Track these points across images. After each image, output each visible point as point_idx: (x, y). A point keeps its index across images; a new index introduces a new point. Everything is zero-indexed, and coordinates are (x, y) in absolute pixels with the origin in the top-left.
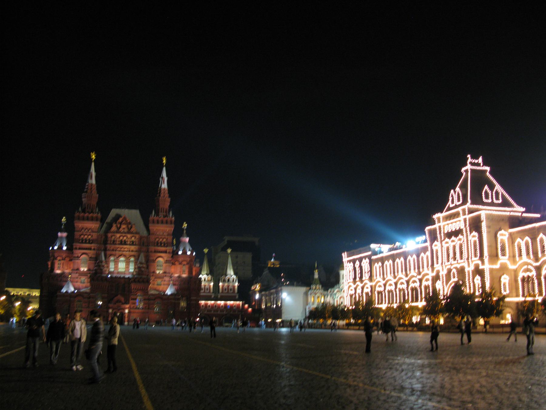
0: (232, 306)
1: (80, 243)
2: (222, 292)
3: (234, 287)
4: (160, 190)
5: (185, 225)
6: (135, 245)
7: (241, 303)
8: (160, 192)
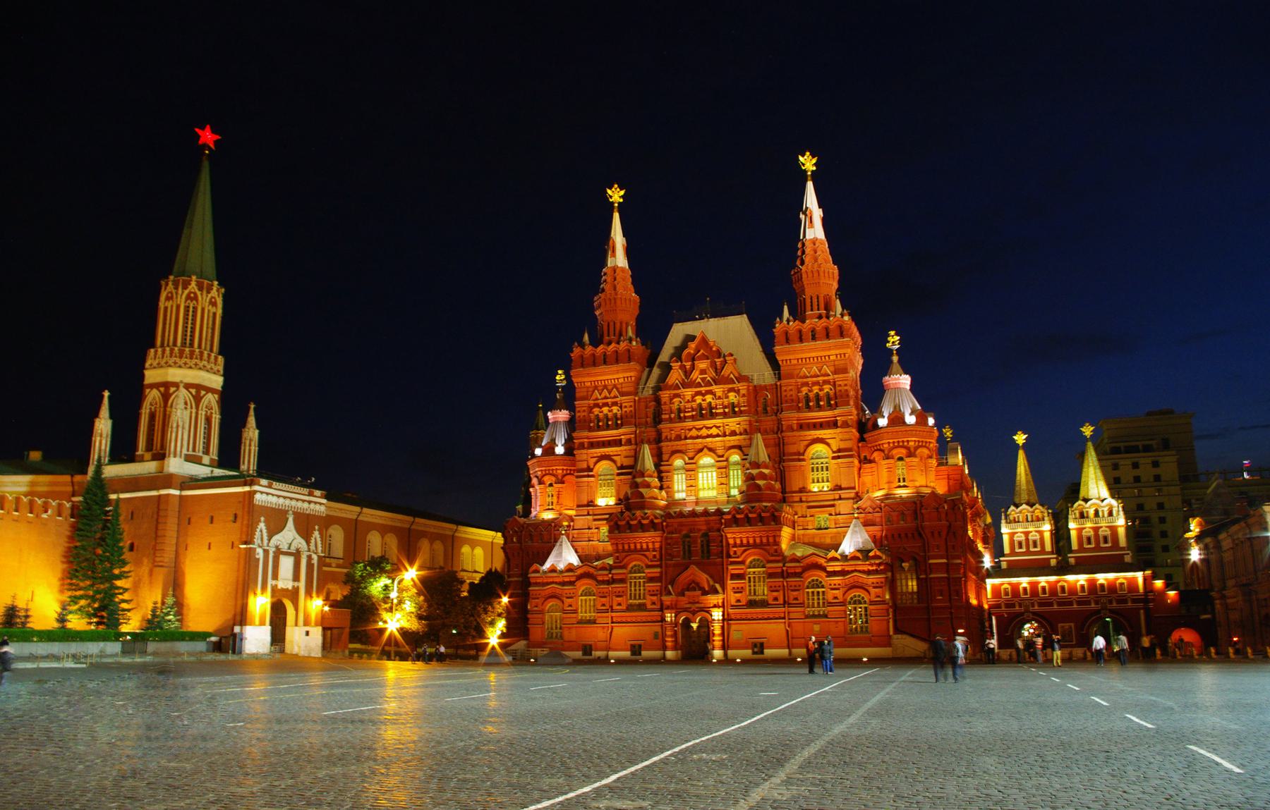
0: (1112, 588)
1: (590, 429)
2: (1081, 549)
3: (1113, 529)
4: (803, 245)
5: (894, 340)
6: (741, 413)
7: (1139, 576)
8: (803, 252)
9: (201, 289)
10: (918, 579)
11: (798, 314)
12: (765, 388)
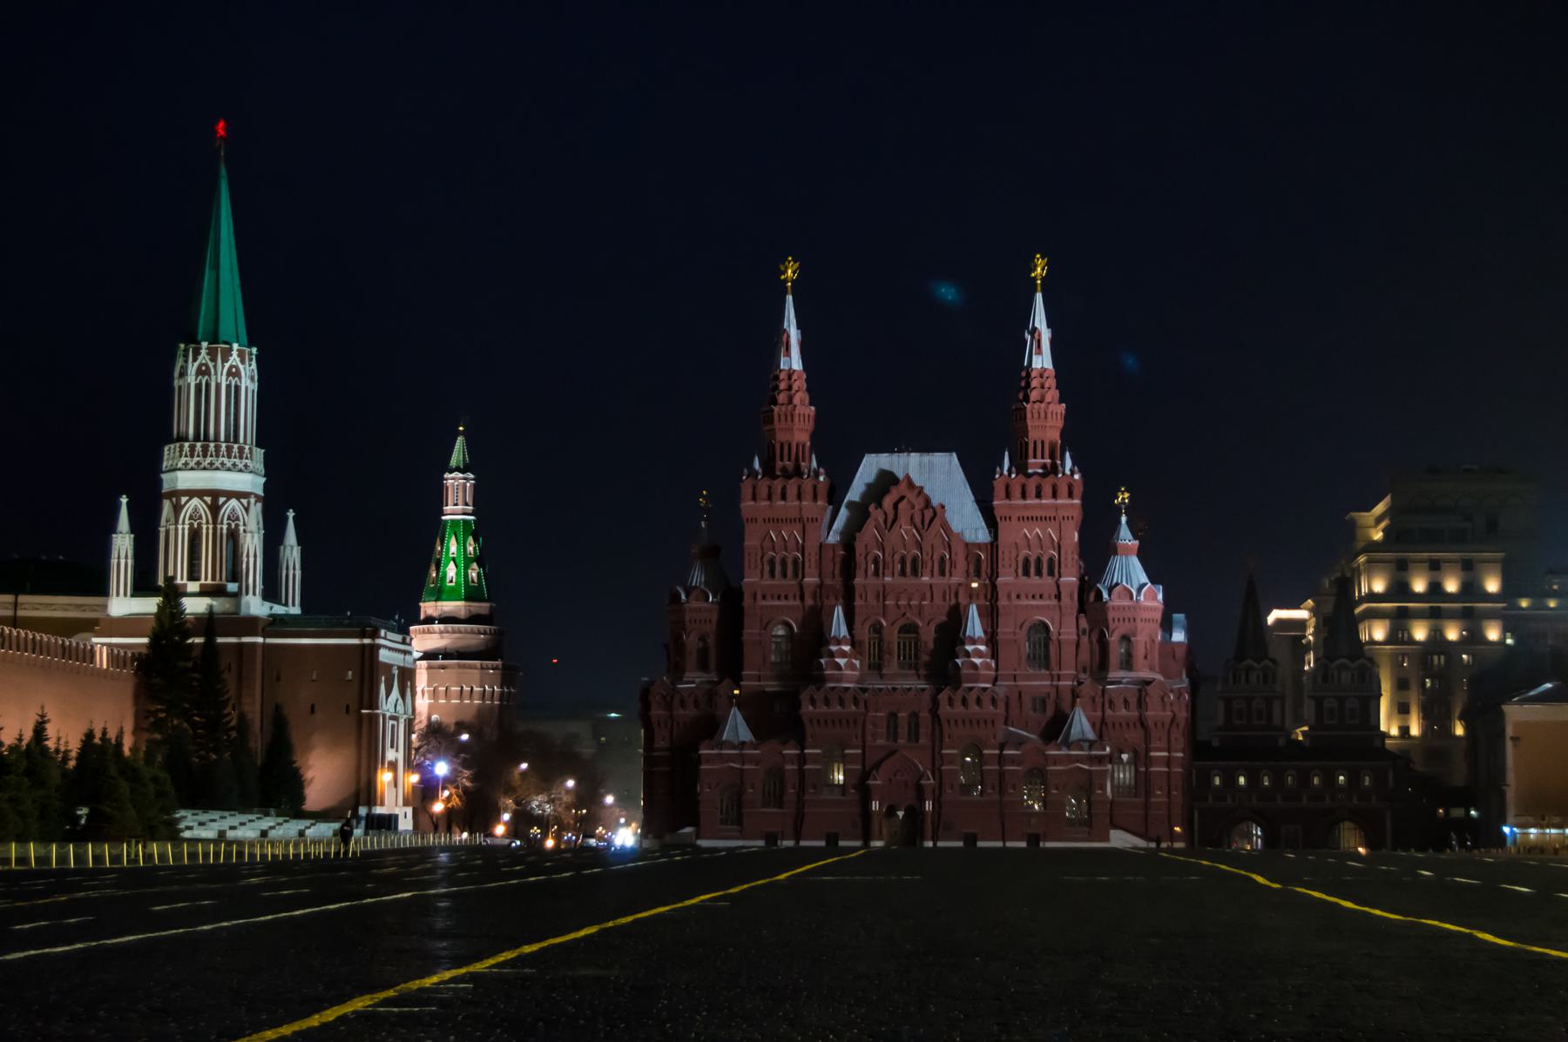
4: (1028, 375)
8: (1028, 385)
9: (243, 362)
10: (1137, 771)
12: (979, 546)
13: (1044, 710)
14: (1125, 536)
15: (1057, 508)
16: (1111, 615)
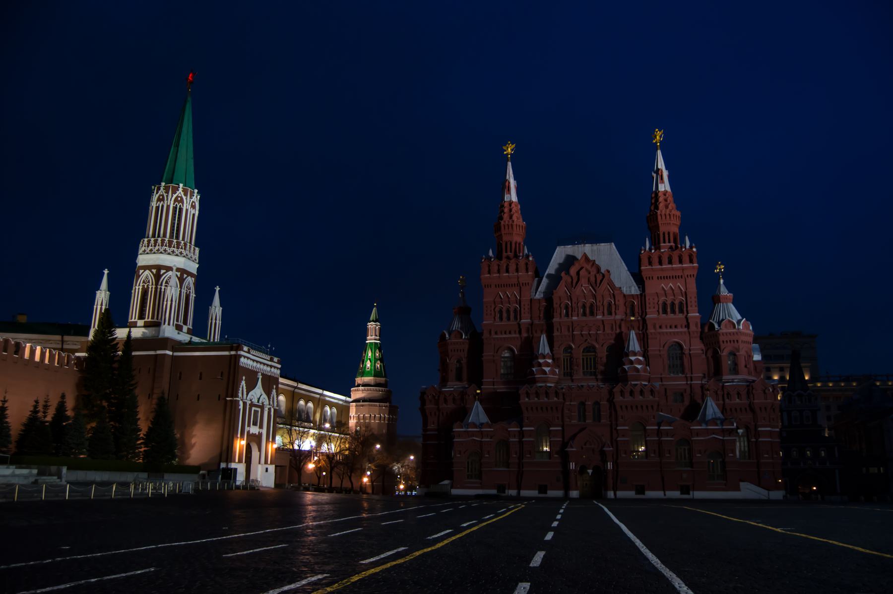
9: (186, 195)
10: (749, 441)
11: (655, 244)
13: (683, 401)
14: (724, 291)
15: (683, 269)
16: (721, 338)
